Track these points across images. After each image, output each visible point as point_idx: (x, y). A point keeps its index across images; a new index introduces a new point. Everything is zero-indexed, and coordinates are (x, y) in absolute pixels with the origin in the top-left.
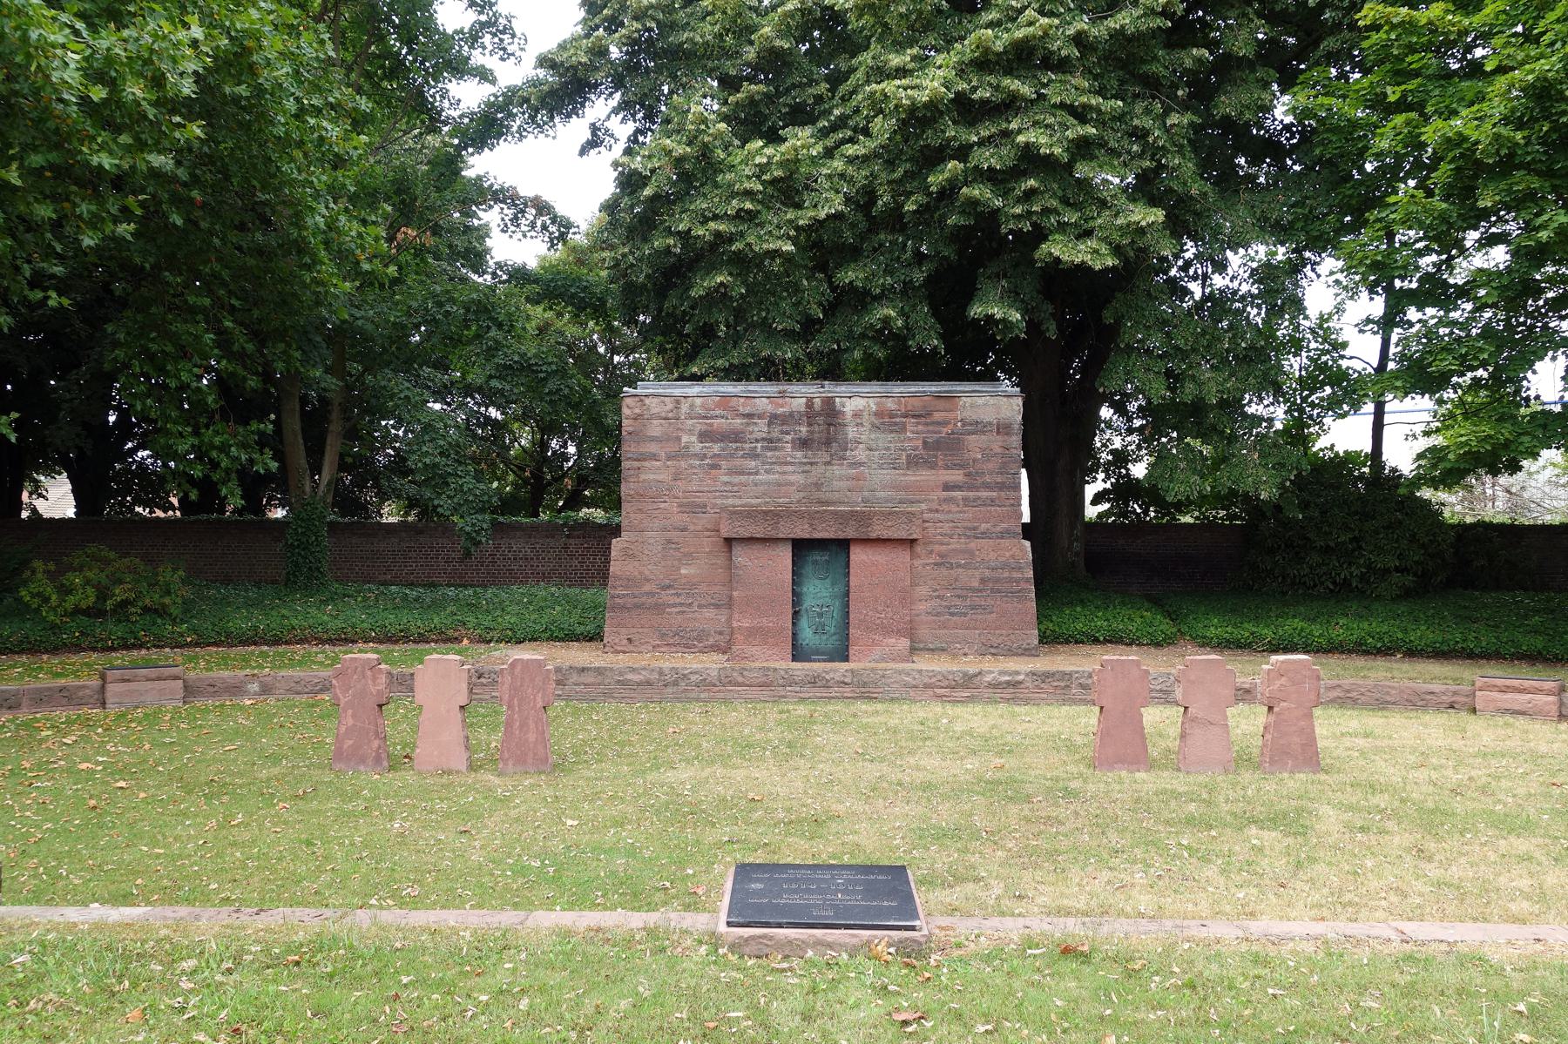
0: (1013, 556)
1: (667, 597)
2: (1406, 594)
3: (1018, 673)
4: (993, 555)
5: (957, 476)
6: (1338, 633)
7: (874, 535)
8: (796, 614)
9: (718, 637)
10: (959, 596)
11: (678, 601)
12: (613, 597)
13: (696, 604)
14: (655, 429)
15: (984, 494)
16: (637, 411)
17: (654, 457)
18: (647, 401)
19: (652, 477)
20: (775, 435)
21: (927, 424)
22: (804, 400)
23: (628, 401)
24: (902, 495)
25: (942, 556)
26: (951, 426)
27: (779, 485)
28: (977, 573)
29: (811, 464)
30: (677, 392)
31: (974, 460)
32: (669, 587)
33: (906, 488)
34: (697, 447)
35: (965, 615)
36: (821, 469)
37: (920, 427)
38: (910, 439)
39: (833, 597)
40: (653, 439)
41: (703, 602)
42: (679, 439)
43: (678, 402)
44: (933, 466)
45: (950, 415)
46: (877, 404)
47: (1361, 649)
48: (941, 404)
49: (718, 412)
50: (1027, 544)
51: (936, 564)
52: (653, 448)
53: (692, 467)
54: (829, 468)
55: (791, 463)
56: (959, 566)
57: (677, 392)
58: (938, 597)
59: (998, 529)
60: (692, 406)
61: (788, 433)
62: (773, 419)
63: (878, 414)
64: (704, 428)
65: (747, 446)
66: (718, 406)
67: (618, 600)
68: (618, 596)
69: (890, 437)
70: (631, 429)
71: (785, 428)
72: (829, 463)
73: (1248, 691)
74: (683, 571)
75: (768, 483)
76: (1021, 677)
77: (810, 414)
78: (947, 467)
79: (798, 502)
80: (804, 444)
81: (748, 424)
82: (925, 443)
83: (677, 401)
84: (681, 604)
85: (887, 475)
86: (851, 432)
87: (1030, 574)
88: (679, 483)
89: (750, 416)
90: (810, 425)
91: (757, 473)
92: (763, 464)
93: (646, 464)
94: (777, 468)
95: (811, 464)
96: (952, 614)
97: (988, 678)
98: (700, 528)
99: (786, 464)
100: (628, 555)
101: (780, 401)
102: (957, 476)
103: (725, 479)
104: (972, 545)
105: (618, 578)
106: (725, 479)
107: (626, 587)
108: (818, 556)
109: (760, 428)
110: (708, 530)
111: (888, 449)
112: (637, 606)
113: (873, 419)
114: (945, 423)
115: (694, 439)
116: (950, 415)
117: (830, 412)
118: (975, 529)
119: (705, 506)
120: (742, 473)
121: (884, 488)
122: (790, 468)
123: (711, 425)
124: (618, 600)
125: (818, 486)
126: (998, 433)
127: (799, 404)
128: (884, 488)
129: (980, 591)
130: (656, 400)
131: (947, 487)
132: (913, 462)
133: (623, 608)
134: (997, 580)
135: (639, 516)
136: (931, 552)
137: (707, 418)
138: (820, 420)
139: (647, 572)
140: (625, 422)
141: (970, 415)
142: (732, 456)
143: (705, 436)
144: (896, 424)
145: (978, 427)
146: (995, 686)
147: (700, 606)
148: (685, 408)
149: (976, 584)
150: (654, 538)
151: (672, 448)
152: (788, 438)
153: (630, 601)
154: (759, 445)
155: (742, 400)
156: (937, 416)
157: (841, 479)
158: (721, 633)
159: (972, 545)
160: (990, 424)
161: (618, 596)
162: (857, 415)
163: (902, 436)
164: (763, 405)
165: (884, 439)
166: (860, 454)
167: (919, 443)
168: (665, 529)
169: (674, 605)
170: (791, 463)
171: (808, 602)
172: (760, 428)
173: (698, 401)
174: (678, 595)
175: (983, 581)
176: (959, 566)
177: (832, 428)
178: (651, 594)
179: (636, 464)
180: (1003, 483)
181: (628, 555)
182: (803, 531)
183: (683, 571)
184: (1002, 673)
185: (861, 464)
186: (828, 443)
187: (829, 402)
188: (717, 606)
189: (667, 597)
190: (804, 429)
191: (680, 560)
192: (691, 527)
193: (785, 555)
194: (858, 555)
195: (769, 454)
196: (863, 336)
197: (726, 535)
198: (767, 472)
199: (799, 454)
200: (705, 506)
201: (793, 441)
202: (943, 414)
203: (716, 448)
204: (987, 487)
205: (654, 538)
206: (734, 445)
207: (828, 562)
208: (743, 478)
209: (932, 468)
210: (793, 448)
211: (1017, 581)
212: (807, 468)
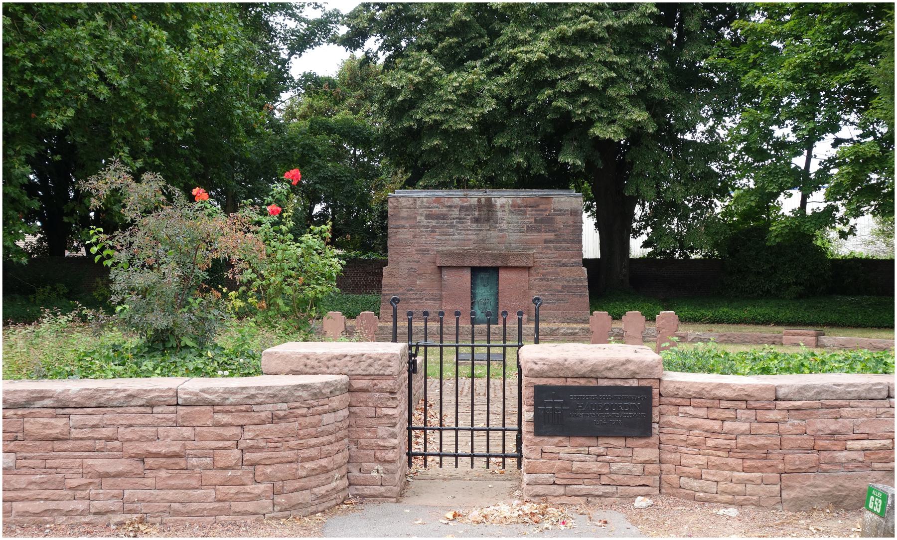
0: (578, 275)
1: (410, 295)
2: (800, 296)
3: (576, 329)
4: (568, 275)
5: (551, 236)
6: (745, 314)
7: (510, 265)
8: (473, 304)
11: (415, 297)
14: (404, 213)
15: (564, 245)
16: (395, 204)
17: (404, 227)
18: (400, 200)
19: (402, 236)
20: (463, 216)
21: (536, 211)
23: (391, 199)
24: (524, 245)
25: (543, 275)
26: (548, 212)
27: (464, 240)
28: (561, 283)
29: (480, 230)
30: (415, 195)
31: (560, 228)
32: (411, 290)
33: (526, 242)
34: (425, 222)
35: (555, 303)
36: (485, 232)
37: (533, 212)
38: (529, 218)
39: (490, 295)
40: (403, 218)
41: (428, 297)
42: (416, 218)
43: (415, 200)
44: (539, 231)
45: (548, 206)
46: (512, 201)
47: (755, 322)
48: (544, 201)
49: (435, 205)
50: (585, 269)
52: (403, 222)
53: (422, 232)
55: (470, 230)
56: (552, 280)
59: (571, 262)
60: (422, 202)
62: (462, 208)
63: (513, 206)
64: (428, 213)
65: (449, 221)
66: (435, 202)
69: (518, 217)
70: (392, 213)
71: (468, 213)
72: (488, 230)
73: (683, 337)
74: (418, 282)
75: (459, 240)
76: (577, 331)
77: (480, 206)
78: (546, 232)
79: (474, 249)
80: (476, 220)
81: (449, 211)
82: (536, 220)
83: (415, 199)
84: (417, 299)
85: (516, 236)
86: (500, 215)
87: (586, 284)
89: (450, 207)
91: (454, 235)
92: (457, 230)
93: (400, 230)
94: (463, 232)
95: (480, 230)
97: (562, 331)
98: (426, 261)
99: (468, 230)
100: (391, 274)
101: (465, 199)
102: (551, 236)
103: (438, 237)
104: (558, 270)
105: (386, 286)
106: (438, 237)
107: (390, 290)
108: (483, 275)
109: (456, 213)
111: (517, 223)
113: (510, 208)
114: (545, 210)
115: (423, 218)
116: (548, 206)
117: (490, 205)
118: (559, 262)
119: (429, 251)
120: (446, 235)
121: (515, 242)
122: (470, 232)
123: (431, 211)
125: (483, 241)
126: (571, 215)
127: (474, 201)
128: (515, 242)
129: (562, 292)
130: (404, 199)
131: (546, 241)
132: (530, 229)
134: (570, 287)
135: (396, 256)
136: (538, 273)
138: (485, 209)
139: (400, 283)
140: (389, 210)
141: (557, 206)
142: (441, 226)
143: (428, 217)
144: (521, 211)
145: (562, 212)
146: (563, 334)
148: (418, 203)
149: (560, 289)
150: (404, 266)
151: (411, 222)
152: (469, 217)
156: (542, 207)
157: (494, 238)
159: (558, 270)
160: (567, 210)
162: (502, 206)
163: (524, 217)
164: (456, 201)
165: (515, 218)
166: (504, 225)
167: (533, 220)
168: (409, 262)
169: (414, 299)
170: (470, 230)
171: (479, 298)
172: (456, 213)
173: (425, 200)
174: (416, 294)
175: (563, 287)
176: (552, 280)
178: (402, 294)
179: (395, 230)
180: (573, 239)
181: (391, 274)
182: (476, 263)
183: (418, 282)
184: (568, 329)
185: (504, 230)
186: (488, 220)
187: (489, 200)
188: (434, 300)
189: (410, 295)
190: (476, 213)
192: (422, 261)
193: (467, 275)
194: (503, 275)
195: (460, 225)
197: (439, 265)
198: (458, 234)
199: (474, 225)
200: (429, 251)
201: (471, 219)
202: (545, 206)
203: (434, 222)
204: (566, 241)
205: (404, 266)
206: (442, 221)
207: (488, 278)
208: (447, 237)
209: (539, 232)
211: (580, 287)
212: (478, 232)
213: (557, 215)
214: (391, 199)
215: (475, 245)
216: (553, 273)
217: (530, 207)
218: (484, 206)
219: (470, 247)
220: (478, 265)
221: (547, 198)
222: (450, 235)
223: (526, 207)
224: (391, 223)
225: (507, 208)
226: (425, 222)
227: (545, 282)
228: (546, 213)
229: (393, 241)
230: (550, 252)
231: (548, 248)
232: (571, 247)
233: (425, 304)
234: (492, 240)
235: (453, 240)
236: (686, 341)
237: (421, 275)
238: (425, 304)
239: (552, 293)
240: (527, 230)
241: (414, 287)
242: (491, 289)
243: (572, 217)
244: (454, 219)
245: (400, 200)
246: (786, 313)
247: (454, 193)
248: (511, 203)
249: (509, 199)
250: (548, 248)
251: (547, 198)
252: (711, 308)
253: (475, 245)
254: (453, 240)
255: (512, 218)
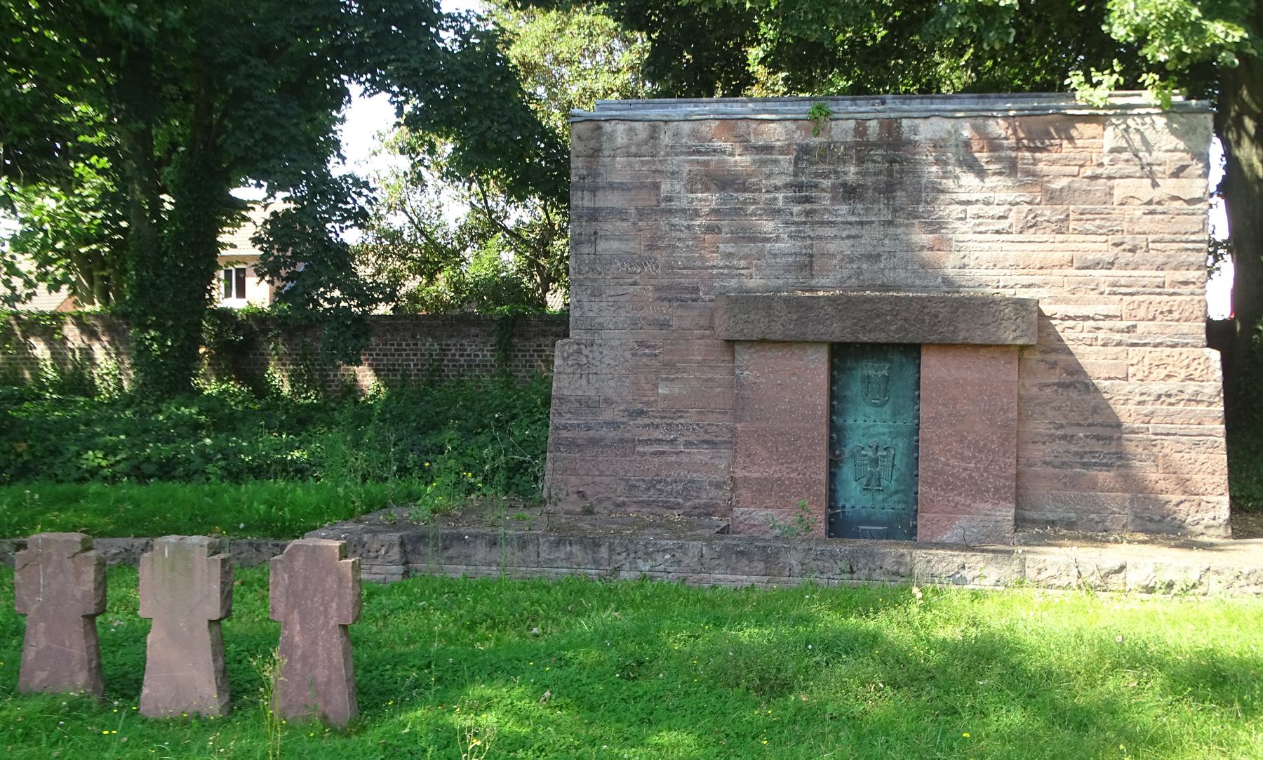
1: (636, 427)
7: (960, 338)
8: (834, 464)
9: (714, 493)
10: (1098, 438)
12: (557, 428)
13: (681, 440)
17: (620, 214)
18: (608, 127)
22: (852, 123)
32: (641, 413)
36: (876, 232)
39: (895, 434)
41: (692, 438)
42: (656, 186)
51: (1060, 385)
54: (891, 230)
57: (654, 113)
58: (1064, 437)
61: (825, 176)
64: (695, 168)
67: (564, 434)
68: (565, 428)
71: (822, 167)
72: (890, 223)
77: (861, 149)
80: (850, 193)
88: (657, 254)
90: (861, 161)
91: (778, 239)
95: (861, 223)
96: (1085, 465)
103: (730, 248)
105: (562, 399)
106: (730, 248)
108: (871, 369)
110: (701, 328)
112: (593, 442)
122: (829, 232)
123: (706, 163)
124: (564, 434)
127: (842, 130)
133: (572, 444)
136: (1054, 365)
137: (698, 153)
147: (688, 444)
148: (666, 139)
151: (646, 200)
152: (826, 183)
153: (583, 434)
154: (780, 196)
155: (754, 125)
158: (718, 486)
161: (565, 428)
162: (938, 145)
169: (648, 442)
171: (855, 441)
173: (686, 127)
177: (896, 167)
178: (614, 425)
182: (838, 331)
186: (889, 190)
187: (891, 126)
188: (712, 444)
189: (636, 427)
191: (658, 372)
192: (675, 323)
193: (817, 363)
194: (934, 367)
197: (725, 335)
199: (843, 209)
201: (834, 187)
207: (887, 379)
210: (833, 199)
218: (876, 145)
237: (670, 365)
242: (895, 414)
244: (777, 189)
254: (775, 256)
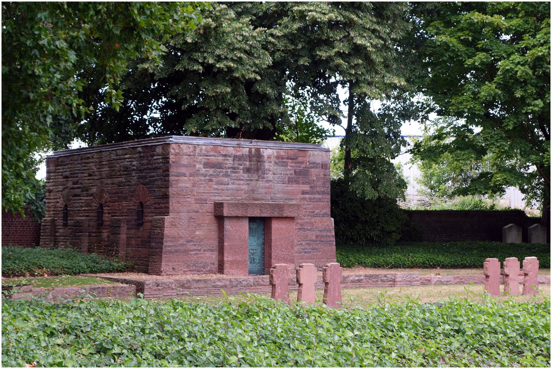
0: (328, 225)
1: (190, 246)
2: (398, 242)
3: (361, 276)
4: (320, 225)
5: (306, 188)
7: (285, 215)
9: (212, 266)
10: (308, 244)
11: (195, 248)
12: (166, 247)
13: (203, 249)
14: (185, 160)
15: (317, 196)
16: (177, 151)
18: (181, 146)
19: (183, 185)
20: (236, 166)
21: (296, 163)
22: (248, 149)
23: (173, 146)
24: (286, 196)
25: (301, 225)
26: (304, 164)
27: (237, 190)
28: (314, 233)
29: (251, 180)
30: (195, 142)
31: (314, 181)
32: (191, 241)
33: (288, 193)
34: (203, 171)
35: (310, 252)
36: (254, 183)
37: (293, 164)
38: (290, 170)
39: (258, 245)
40: (184, 166)
41: (206, 249)
42: (195, 166)
43: (195, 147)
44: (298, 183)
45: (304, 159)
46: (277, 152)
47: (424, 266)
48: (301, 154)
49: (212, 153)
50: (333, 219)
51: (299, 229)
52: (183, 170)
53: (201, 180)
54: (258, 182)
55: (242, 180)
56: (308, 230)
57: (195, 142)
58: (300, 244)
59: (322, 213)
60: (201, 150)
61: (241, 165)
62: (235, 157)
63: (278, 157)
64: (206, 161)
65: (224, 170)
66: (212, 150)
67: (168, 248)
68: (168, 246)
69: (282, 168)
70: (174, 160)
71: (240, 162)
72: (257, 180)
73: (429, 281)
74: (197, 233)
75: (233, 189)
76: (362, 278)
77: (250, 156)
78: (303, 184)
79: (245, 199)
80: (248, 170)
81: (225, 160)
82: (295, 172)
83: (195, 146)
84: (196, 250)
85: (279, 186)
86: (267, 165)
87: (333, 233)
88: (195, 188)
89: (225, 156)
90: (250, 161)
91: (228, 184)
92: (231, 179)
93: (181, 178)
94: (237, 182)
95: (251, 180)
96: (305, 252)
97: (351, 278)
98: (204, 211)
99: (240, 180)
100: (173, 225)
101: (238, 149)
102: (306, 188)
103: (215, 186)
104: (313, 220)
106: (215, 186)
107: (171, 242)
109: (230, 162)
110: (208, 212)
111: (281, 174)
112: (177, 251)
113: (275, 159)
114: (302, 163)
115: (202, 166)
116: (304, 159)
117: (258, 156)
118: (314, 212)
119: (206, 200)
120: (222, 184)
121: (279, 192)
122: (242, 182)
123: (209, 159)
124: (168, 248)
125: (253, 191)
126: (322, 168)
127: (246, 151)
128: (279, 192)
129: (316, 241)
130: (185, 146)
131: (303, 193)
132: (291, 181)
133: (170, 252)
134: (322, 236)
135: (178, 205)
136: (298, 223)
137: (207, 156)
138: (254, 159)
139: (181, 234)
140: (171, 157)
141: (312, 159)
142: (218, 175)
143: (206, 165)
144: (284, 162)
145: (315, 165)
146: (352, 282)
147: (204, 251)
148: (198, 151)
149: (314, 238)
150: (184, 216)
152: (241, 167)
153: (173, 249)
154: (229, 170)
155: (222, 148)
156: (300, 159)
157: (262, 188)
158: (213, 264)
159: (313, 220)
160: (319, 163)
161: (168, 246)
162: (269, 157)
163: (286, 168)
164: (231, 151)
165: (279, 169)
166: (270, 176)
167: (293, 172)
168: (189, 212)
169: (193, 250)
170: (242, 180)
172: (230, 162)
173: (204, 147)
174: (195, 245)
175: (317, 236)
176: (308, 230)
177: (259, 163)
178: (182, 245)
179: (176, 178)
180: (324, 191)
181: (173, 225)
183: (197, 233)
184: (356, 276)
185: (271, 181)
186: (258, 170)
187: (258, 150)
188: (212, 251)
189: (190, 246)
190: (248, 163)
191: (195, 227)
192: (201, 211)
194: (275, 225)
195: (234, 175)
196: (264, 118)
198: (233, 184)
199: (246, 175)
200: (206, 200)
201: (243, 169)
202: (302, 158)
203: (211, 171)
204: (318, 193)
205: (184, 216)
206: (219, 170)
208: (223, 186)
209: (298, 183)
210: (243, 172)
211: (329, 237)
212: (249, 182)
213: (312, 168)
214: (173, 146)
215: (247, 195)
216: (309, 223)
217: (291, 159)
218: (254, 156)
219: (242, 197)
220: (259, 215)
221: (304, 151)
222: (225, 184)
223: (288, 158)
224: (173, 170)
225: (273, 159)
226: (203, 171)
227: (302, 232)
228: (303, 166)
229: (174, 189)
230: (306, 203)
231: (304, 199)
232: (322, 198)
233: (203, 255)
234: (261, 190)
235: (228, 190)
236: (431, 284)
237: (199, 225)
238: (203, 255)
239: (308, 242)
240: (289, 181)
241: (193, 238)
242: (258, 239)
243: (323, 170)
244: (229, 168)
245: (181, 146)
246: (420, 257)
247: (227, 142)
248: (276, 154)
249: (275, 151)
250: (304, 199)
251: (304, 151)
252: (370, 254)
253: (247, 195)
254: (228, 190)
255: (276, 169)
